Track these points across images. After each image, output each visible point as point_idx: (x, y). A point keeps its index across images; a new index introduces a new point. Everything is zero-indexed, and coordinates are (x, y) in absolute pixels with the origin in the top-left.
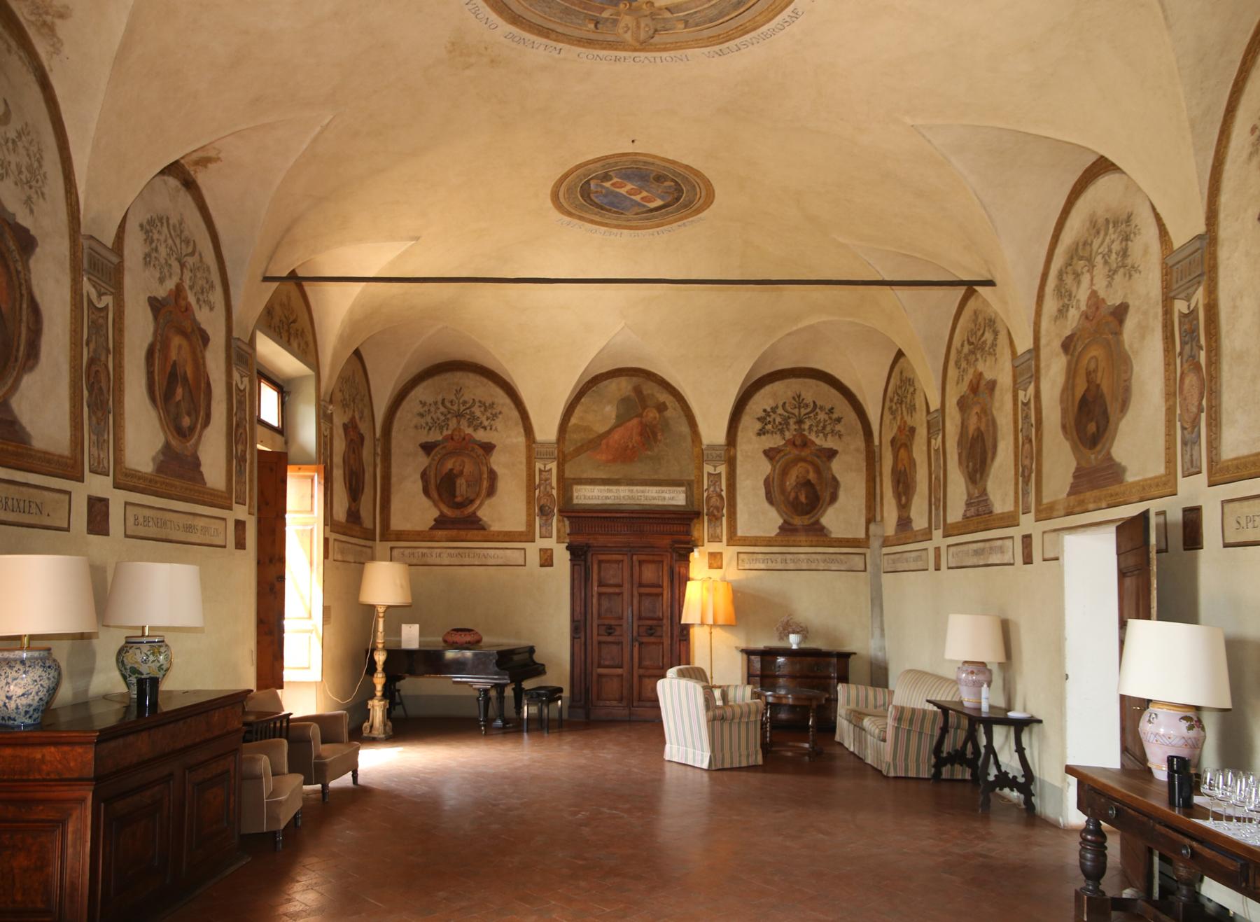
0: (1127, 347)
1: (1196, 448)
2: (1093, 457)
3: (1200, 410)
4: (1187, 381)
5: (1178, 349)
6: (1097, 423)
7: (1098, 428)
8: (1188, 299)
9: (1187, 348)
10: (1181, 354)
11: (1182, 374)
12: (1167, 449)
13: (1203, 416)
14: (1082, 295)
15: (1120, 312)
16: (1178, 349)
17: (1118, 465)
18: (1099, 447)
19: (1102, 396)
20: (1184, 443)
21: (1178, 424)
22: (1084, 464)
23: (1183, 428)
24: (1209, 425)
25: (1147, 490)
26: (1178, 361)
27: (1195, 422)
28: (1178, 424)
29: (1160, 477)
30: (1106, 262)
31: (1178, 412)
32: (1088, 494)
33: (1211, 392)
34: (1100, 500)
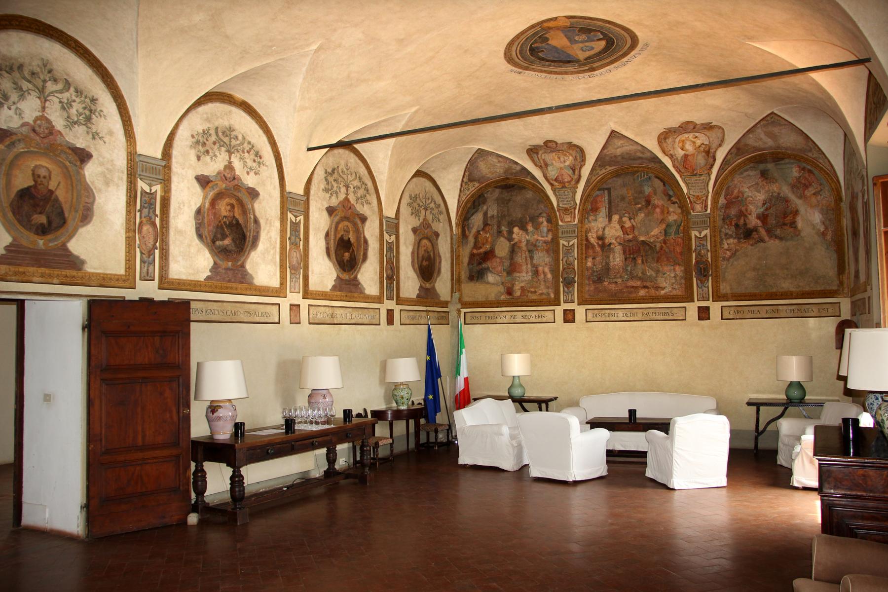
0: (88, 180)
1: (152, 267)
2: (41, 242)
3: (155, 248)
4: (145, 228)
5: (138, 207)
6: (48, 218)
7: (50, 222)
8: (150, 186)
9: (145, 211)
10: (140, 211)
11: (141, 222)
12: (128, 261)
13: (157, 252)
14: (30, 108)
15: (83, 156)
16: (138, 207)
17: (78, 257)
18: (49, 237)
19: (57, 200)
20: (142, 261)
21: (138, 250)
22: (24, 242)
23: (142, 253)
24: (161, 258)
25: (104, 281)
26: (138, 214)
27: (151, 253)
28: (138, 250)
29: (121, 275)
30: (63, 108)
31: (138, 242)
32: (31, 269)
33: (162, 241)
34: (50, 276)
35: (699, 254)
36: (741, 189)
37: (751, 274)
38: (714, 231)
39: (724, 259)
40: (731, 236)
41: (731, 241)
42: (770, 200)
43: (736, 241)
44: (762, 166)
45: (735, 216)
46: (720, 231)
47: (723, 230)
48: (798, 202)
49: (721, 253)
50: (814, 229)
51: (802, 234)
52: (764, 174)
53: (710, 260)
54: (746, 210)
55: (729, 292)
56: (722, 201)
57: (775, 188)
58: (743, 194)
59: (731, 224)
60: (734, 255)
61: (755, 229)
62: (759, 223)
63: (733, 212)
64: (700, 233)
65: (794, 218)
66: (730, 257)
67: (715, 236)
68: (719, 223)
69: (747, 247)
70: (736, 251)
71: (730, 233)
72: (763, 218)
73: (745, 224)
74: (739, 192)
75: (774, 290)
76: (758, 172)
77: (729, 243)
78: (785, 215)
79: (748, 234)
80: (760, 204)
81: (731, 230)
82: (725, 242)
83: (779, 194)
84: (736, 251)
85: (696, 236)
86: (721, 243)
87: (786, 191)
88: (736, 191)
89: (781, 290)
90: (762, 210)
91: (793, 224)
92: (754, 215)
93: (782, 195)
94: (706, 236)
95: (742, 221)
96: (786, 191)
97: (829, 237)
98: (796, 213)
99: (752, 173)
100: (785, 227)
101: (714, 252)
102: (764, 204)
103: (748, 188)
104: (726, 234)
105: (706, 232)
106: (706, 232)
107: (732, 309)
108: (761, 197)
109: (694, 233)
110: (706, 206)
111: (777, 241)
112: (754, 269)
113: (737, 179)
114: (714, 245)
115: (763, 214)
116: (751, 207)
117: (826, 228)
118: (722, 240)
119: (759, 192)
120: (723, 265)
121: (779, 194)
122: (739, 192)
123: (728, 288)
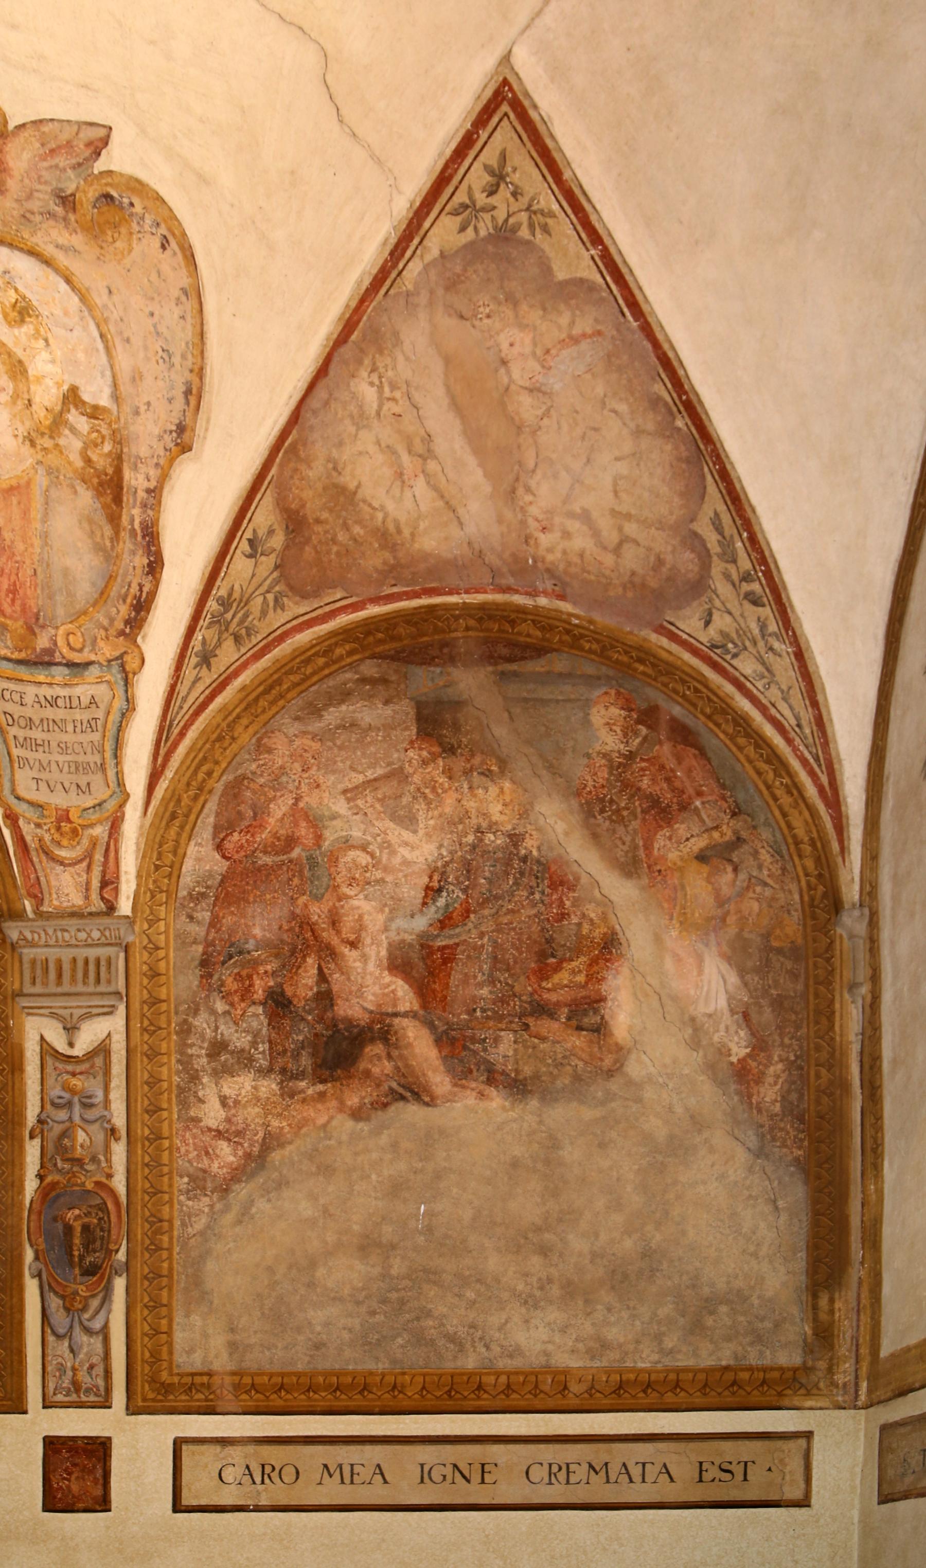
35: (59, 1151)
36: (310, 800)
37: (347, 1273)
38: (151, 1029)
39: (199, 1182)
40: (245, 1060)
41: (242, 1085)
42: (468, 869)
43: (269, 1086)
44: (424, 680)
45: (274, 948)
46: (186, 1030)
47: (201, 1022)
48: (620, 891)
49: (185, 1151)
50: (695, 1043)
51: (634, 1068)
52: (437, 725)
53: (119, 1184)
54: (335, 922)
55: (222, 1362)
56: (200, 859)
57: (493, 803)
58: (316, 823)
59: (246, 993)
60: (255, 1162)
61: (380, 1030)
62: (404, 995)
63: (260, 924)
64: (71, 1029)
65: (594, 977)
66: (237, 1175)
67: (153, 1054)
68: (183, 982)
69: (330, 1121)
70: (271, 1141)
71: (241, 1041)
72: (426, 966)
73: (325, 998)
74: (298, 813)
75: (470, 1362)
76: (405, 709)
77: (233, 1098)
78: (546, 957)
79: (337, 1051)
80: (412, 893)
81: (247, 1028)
82: (209, 1090)
83: (515, 839)
84: (271, 1141)
85: (47, 1050)
86: (187, 1095)
87: (555, 826)
88: (279, 809)
89: (504, 1364)
90: (421, 923)
91: (587, 1013)
92: (376, 951)
93: (530, 845)
94: (103, 1050)
95: (305, 983)
96: (555, 826)
97: (769, 1093)
98: (608, 948)
99: (369, 713)
100: (545, 1026)
101: (149, 1144)
102: (431, 892)
103: (352, 794)
104: (218, 1047)
105: (106, 1028)
106: (106, 1028)
107: (236, 1454)
108: (417, 849)
109: (37, 1031)
110: (109, 882)
111: (497, 1101)
112: (367, 1245)
113: (288, 740)
114: (148, 1100)
115: (425, 944)
116: (362, 906)
117: (759, 1046)
118: (195, 1078)
119: (408, 821)
120: (192, 1213)
121: (515, 839)
122: (298, 813)
123: (218, 1342)
